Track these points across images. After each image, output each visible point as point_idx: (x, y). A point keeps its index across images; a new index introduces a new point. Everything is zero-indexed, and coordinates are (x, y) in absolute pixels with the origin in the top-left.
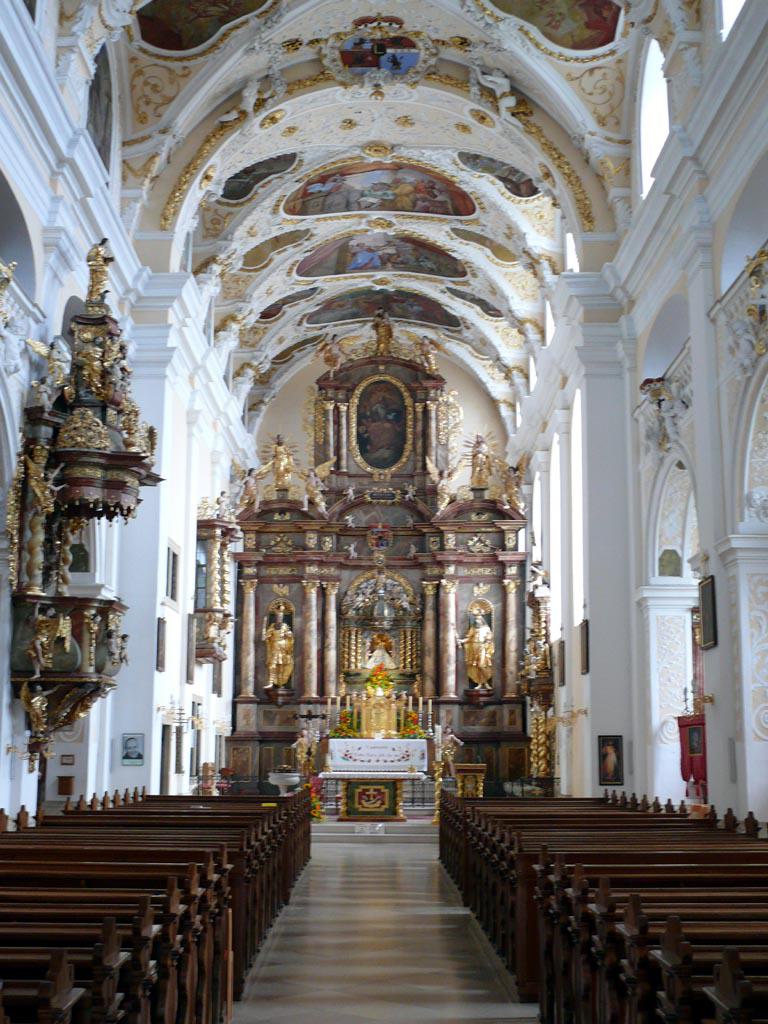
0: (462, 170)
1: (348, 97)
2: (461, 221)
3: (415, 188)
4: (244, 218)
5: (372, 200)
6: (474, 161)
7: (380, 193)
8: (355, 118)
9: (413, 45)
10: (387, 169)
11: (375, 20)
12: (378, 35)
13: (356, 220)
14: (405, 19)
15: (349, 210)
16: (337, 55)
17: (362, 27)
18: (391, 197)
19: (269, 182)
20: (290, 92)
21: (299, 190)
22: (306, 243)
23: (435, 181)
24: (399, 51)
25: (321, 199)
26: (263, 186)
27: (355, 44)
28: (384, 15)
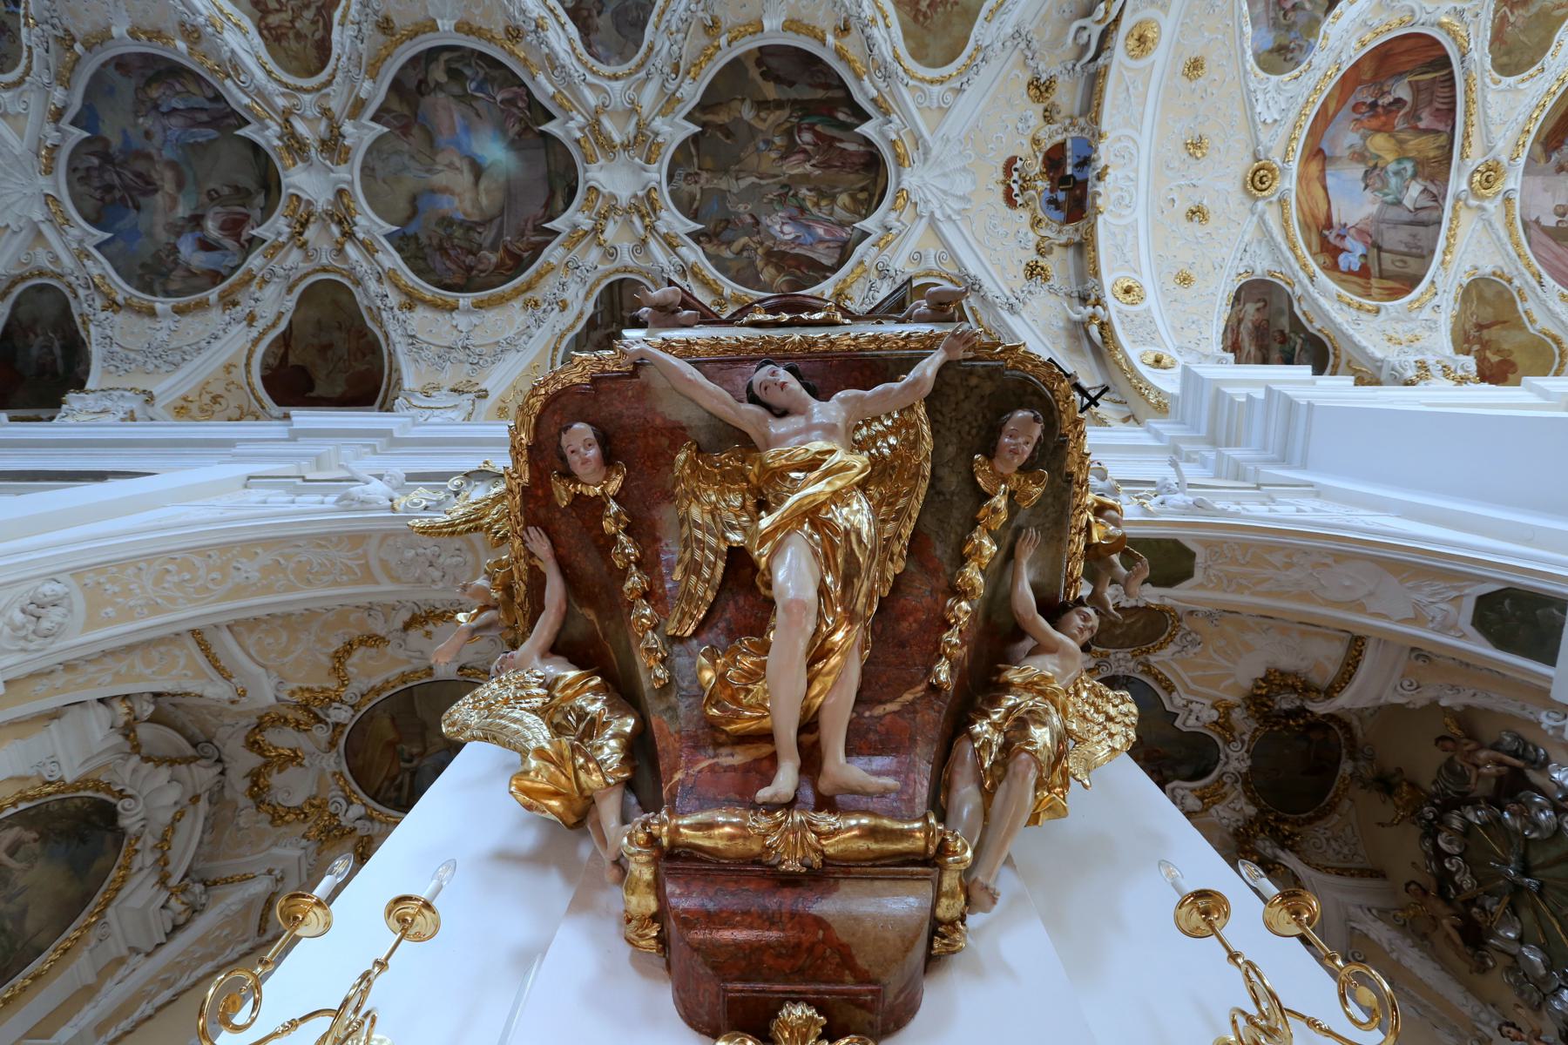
0: (1310, 64)
1: (1126, 212)
2: (1463, 55)
3: (1378, 130)
4: (1355, 345)
5: (1415, 189)
6: (1292, 51)
7: (1393, 181)
8: (1183, 206)
9: (1061, 147)
10: (1323, 170)
11: (1009, 185)
12: (1043, 184)
13: (1464, 215)
14: (1008, 156)
15: (1439, 223)
16: (1069, 227)
17: (1019, 200)
18: (1409, 166)
19: (1304, 313)
20: (1096, 274)
21: (1340, 282)
22: (1517, 282)
23: (1351, 102)
24: (1069, 161)
25: (1384, 255)
26: (1311, 322)
27: (1057, 208)
28: (1001, 177)
